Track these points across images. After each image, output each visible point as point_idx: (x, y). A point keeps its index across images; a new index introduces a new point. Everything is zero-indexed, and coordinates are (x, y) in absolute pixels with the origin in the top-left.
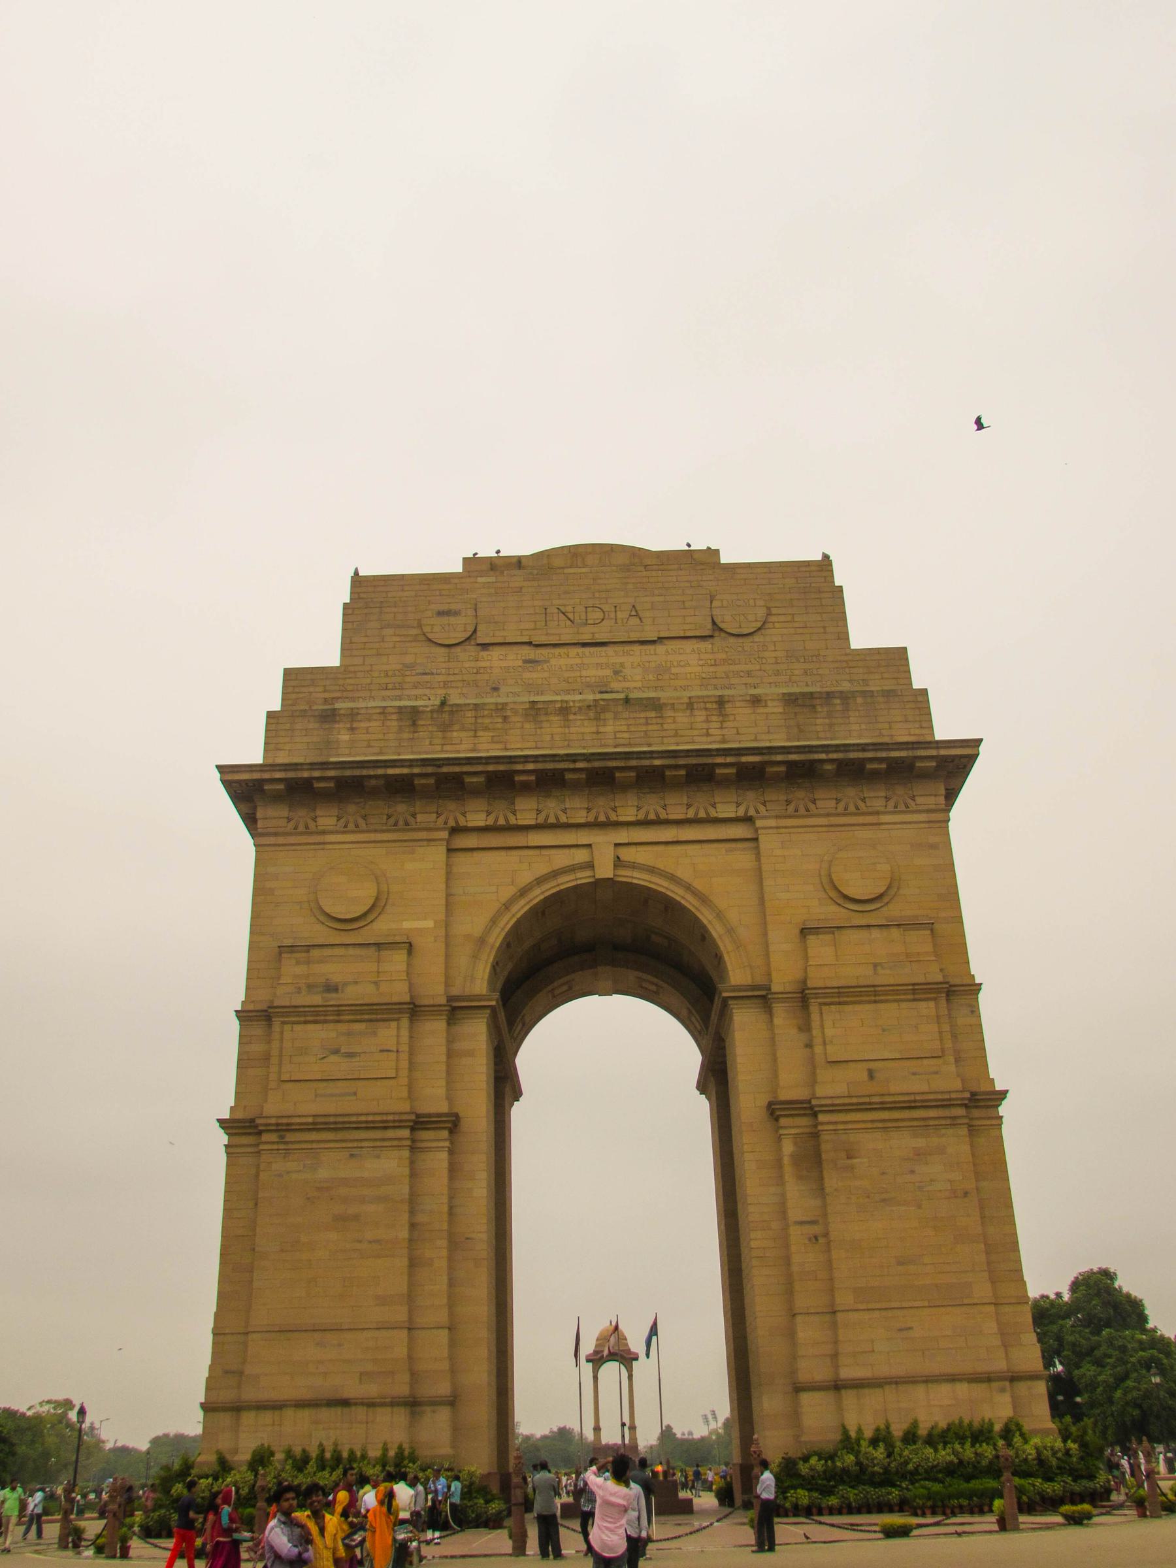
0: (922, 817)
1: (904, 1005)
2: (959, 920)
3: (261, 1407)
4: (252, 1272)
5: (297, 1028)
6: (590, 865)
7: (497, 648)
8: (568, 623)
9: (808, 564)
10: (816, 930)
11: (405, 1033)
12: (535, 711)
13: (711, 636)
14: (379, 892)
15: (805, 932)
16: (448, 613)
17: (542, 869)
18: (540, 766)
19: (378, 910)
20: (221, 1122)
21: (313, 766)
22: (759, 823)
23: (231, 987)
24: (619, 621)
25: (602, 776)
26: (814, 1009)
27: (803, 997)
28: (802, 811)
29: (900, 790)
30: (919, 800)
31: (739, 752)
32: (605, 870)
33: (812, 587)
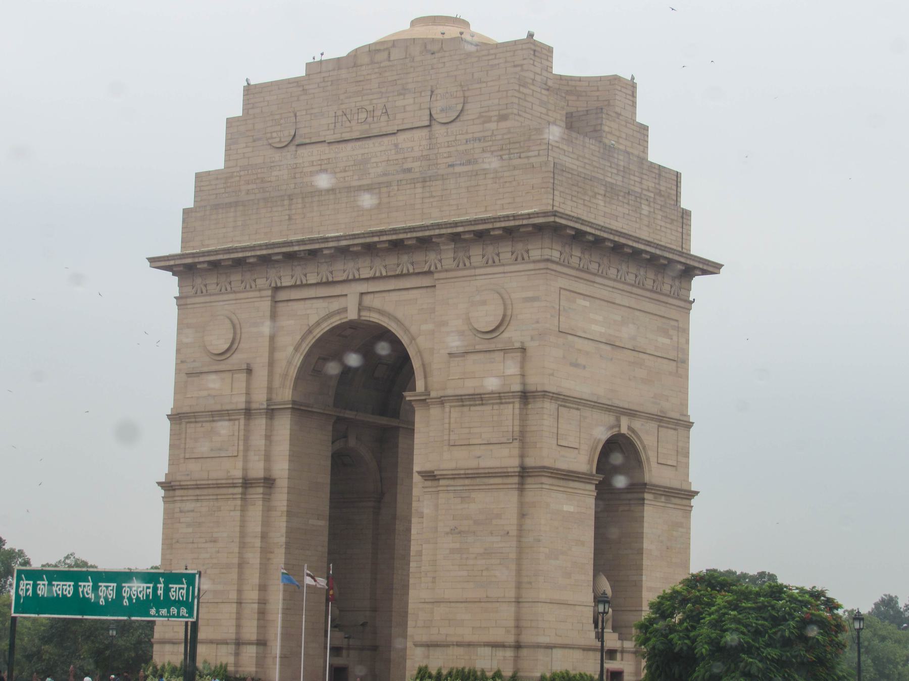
0: (531, 266)
1: (496, 407)
5: (192, 425)
6: (345, 310)
7: (307, 147)
8: (348, 124)
9: (515, 43)
11: (242, 427)
13: (429, 126)
14: (235, 333)
17: (323, 314)
19: (235, 346)
20: (159, 484)
24: (375, 119)
26: (447, 410)
28: (461, 265)
29: (520, 247)
30: (532, 253)
32: (352, 315)
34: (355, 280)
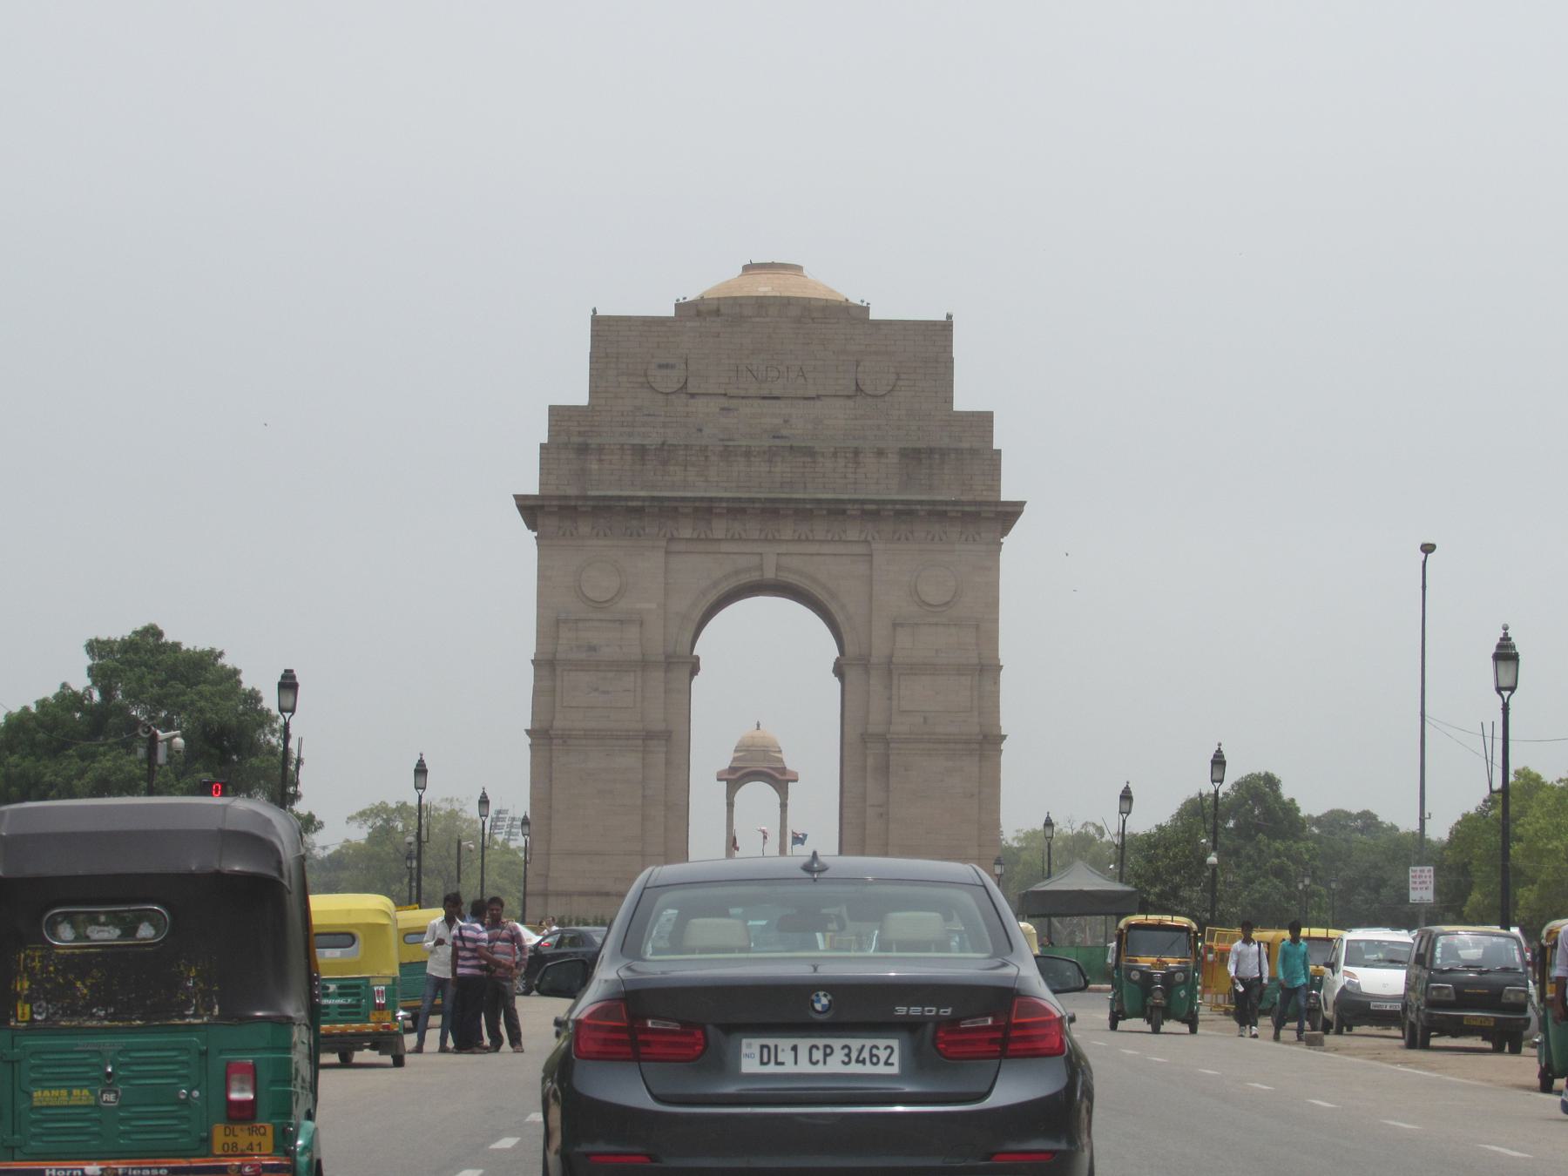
2: (997, 620)
3: (558, 894)
4: (550, 818)
6: (760, 568)
9: (934, 323)
10: (902, 625)
12: (727, 453)
15: (895, 626)
16: (666, 366)
18: (731, 505)
21: (577, 498)
22: (874, 546)
23: (526, 644)
25: (772, 510)
27: (890, 669)
31: (863, 502)
32: (770, 574)
33: (934, 338)
34: (774, 540)
